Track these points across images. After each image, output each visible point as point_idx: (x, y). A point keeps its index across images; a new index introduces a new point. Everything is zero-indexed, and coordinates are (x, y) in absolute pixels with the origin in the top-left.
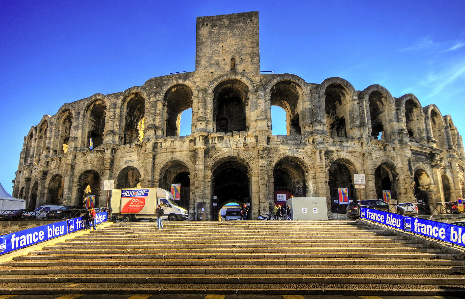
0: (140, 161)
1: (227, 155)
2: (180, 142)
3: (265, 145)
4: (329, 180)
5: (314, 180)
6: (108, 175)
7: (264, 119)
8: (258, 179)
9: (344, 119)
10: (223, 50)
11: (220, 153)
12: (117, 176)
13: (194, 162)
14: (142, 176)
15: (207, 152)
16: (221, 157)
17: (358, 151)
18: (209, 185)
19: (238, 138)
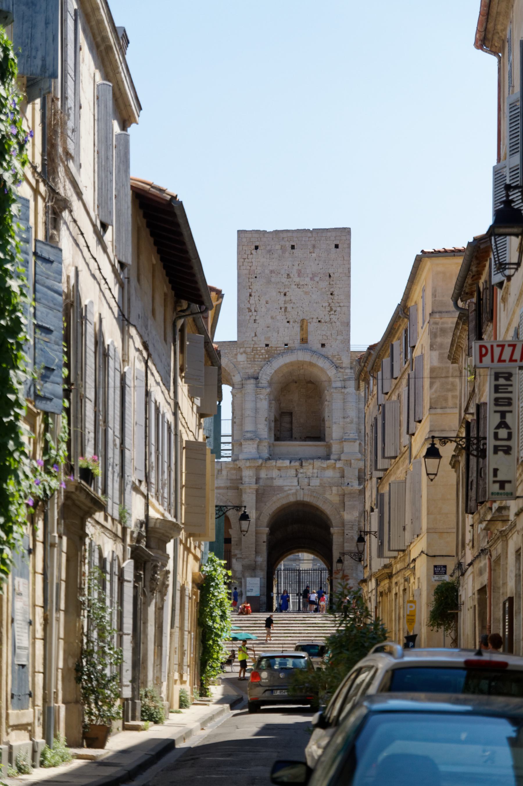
1: (292, 499)
7: (354, 440)
8: (342, 540)
10: (285, 302)
11: (281, 495)
15: (261, 496)
18: (264, 548)
19: (311, 470)
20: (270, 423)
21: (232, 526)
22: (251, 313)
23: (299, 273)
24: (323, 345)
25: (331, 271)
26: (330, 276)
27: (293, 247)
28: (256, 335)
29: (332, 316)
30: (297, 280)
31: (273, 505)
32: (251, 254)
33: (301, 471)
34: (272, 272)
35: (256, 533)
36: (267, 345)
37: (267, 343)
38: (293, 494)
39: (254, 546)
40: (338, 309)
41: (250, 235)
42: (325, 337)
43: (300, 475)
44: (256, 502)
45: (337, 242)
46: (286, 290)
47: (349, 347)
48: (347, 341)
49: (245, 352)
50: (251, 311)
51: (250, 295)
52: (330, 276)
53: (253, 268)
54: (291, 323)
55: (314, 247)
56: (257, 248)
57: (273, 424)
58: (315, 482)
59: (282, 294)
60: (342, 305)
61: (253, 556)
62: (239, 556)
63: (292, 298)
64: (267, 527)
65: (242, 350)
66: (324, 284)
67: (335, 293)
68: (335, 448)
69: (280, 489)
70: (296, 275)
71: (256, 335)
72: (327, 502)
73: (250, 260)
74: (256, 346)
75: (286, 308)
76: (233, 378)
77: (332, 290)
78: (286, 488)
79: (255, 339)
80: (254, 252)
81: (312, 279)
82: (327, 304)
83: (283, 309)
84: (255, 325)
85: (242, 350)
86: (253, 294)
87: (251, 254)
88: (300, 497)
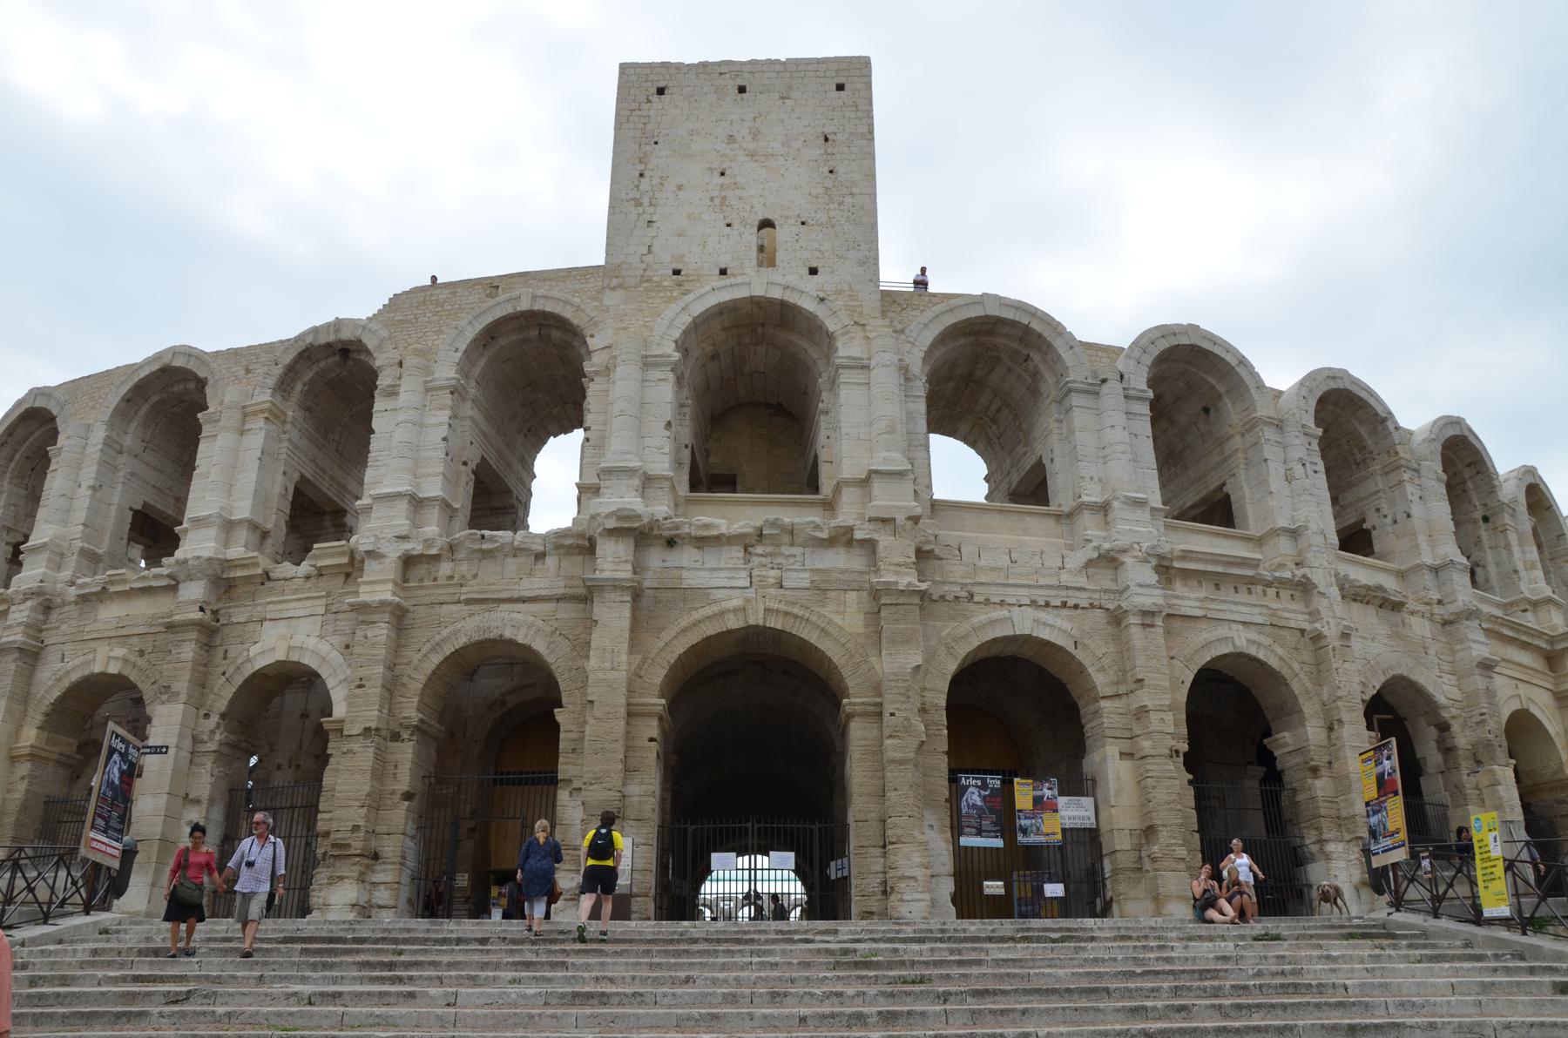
0: (336, 640)
1: (734, 623)
2: (521, 560)
3: (908, 579)
4: (1185, 747)
5: (1125, 746)
6: (183, 697)
8: (875, 733)
9: (1228, 496)
11: (708, 611)
12: (222, 704)
13: (582, 647)
14: (339, 710)
16: (711, 629)
17: (1292, 625)
18: (650, 758)
20: (678, 451)
21: (564, 701)
22: (640, 210)
23: (755, 135)
24: (813, 271)
25: (827, 130)
26: (826, 139)
27: (742, 90)
28: (650, 252)
29: (832, 214)
30: (752, 146)
31: (676, 639)
32: (649, 101)
33: (759, 550)
34: (692, 132)
35: (630, 715)
36: (677, 272)
37: (678, 267)
38: (735, 611)
39: (620, 747)
40: (848, 200)
41: (648, 71)
42: (818, 254)
43: (756, 560)
44: (632, 631)
45: (842, 80)
46: (726, 165)
47: (875, 279)
48: (871, 262)
49: (621, 286)
50: (641, 204)
51: (641, 175)
52: (826, 139)
53: (649, 126)
54: (736, 226)
55: (790, 88)
56: (661, 91)
57: (687, 454)
58: (798, 579)
59: (717, 173)
60: (854, 190)
61: (617, 778)
62: (576, 784)
63: (739, 179)
64: (662, 696)
65: (614, 282)
66: (816, 151)
67: (841, 169)
68: (849, 496)
69: (702, 593)
70: (749, 138)
71: (650, 252)
72: (835, 628)
73: (645, 113)
74: (649, 273)
75: (724, 198)
76: (589, 340)
77: (831, 164)
78: (720, 594)
79: (649, 259)
80: (655, 98)
81: (783, 144)
82: (821, 191)
83: (717, 201)
84: (652, 232)
85: (614, 282)
86: (647, 173)
87: (649, 101)
88: (756, 618)
